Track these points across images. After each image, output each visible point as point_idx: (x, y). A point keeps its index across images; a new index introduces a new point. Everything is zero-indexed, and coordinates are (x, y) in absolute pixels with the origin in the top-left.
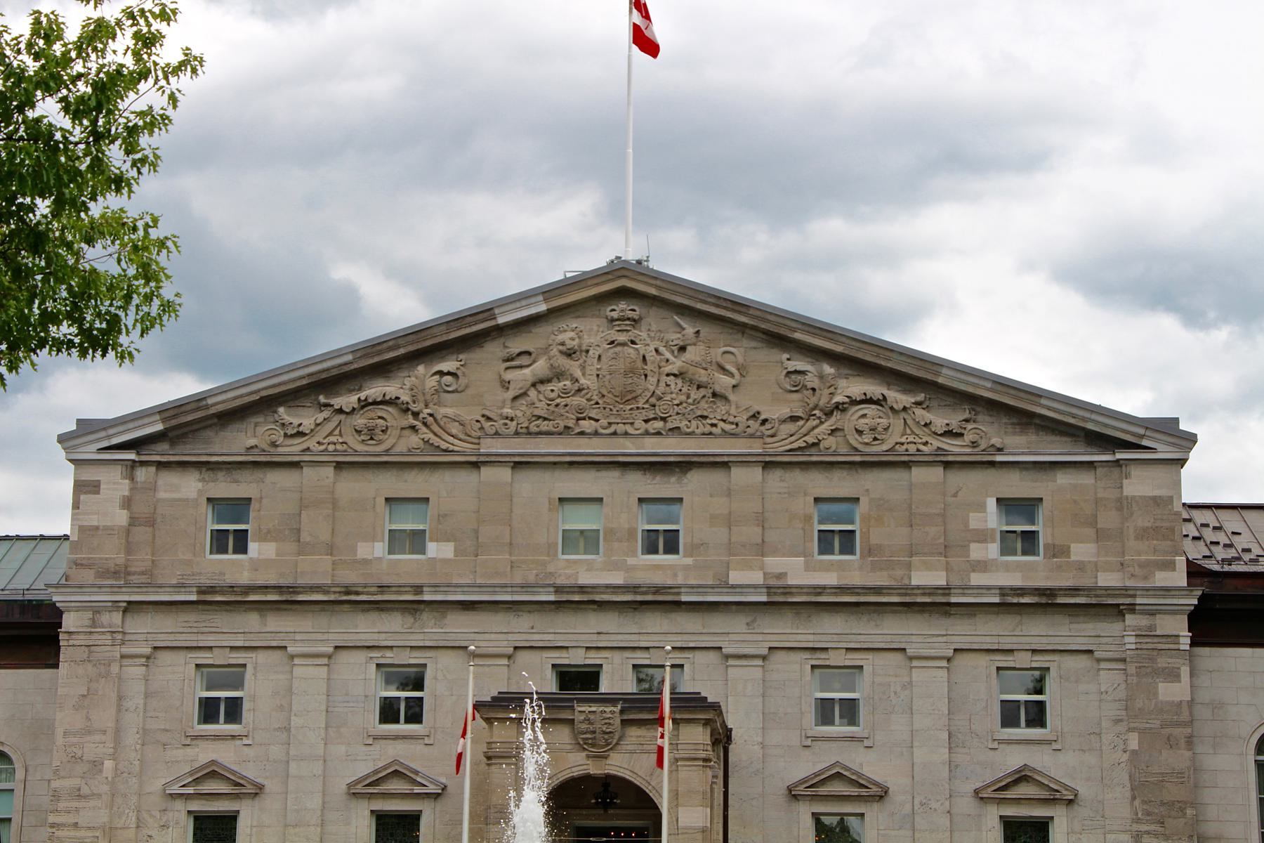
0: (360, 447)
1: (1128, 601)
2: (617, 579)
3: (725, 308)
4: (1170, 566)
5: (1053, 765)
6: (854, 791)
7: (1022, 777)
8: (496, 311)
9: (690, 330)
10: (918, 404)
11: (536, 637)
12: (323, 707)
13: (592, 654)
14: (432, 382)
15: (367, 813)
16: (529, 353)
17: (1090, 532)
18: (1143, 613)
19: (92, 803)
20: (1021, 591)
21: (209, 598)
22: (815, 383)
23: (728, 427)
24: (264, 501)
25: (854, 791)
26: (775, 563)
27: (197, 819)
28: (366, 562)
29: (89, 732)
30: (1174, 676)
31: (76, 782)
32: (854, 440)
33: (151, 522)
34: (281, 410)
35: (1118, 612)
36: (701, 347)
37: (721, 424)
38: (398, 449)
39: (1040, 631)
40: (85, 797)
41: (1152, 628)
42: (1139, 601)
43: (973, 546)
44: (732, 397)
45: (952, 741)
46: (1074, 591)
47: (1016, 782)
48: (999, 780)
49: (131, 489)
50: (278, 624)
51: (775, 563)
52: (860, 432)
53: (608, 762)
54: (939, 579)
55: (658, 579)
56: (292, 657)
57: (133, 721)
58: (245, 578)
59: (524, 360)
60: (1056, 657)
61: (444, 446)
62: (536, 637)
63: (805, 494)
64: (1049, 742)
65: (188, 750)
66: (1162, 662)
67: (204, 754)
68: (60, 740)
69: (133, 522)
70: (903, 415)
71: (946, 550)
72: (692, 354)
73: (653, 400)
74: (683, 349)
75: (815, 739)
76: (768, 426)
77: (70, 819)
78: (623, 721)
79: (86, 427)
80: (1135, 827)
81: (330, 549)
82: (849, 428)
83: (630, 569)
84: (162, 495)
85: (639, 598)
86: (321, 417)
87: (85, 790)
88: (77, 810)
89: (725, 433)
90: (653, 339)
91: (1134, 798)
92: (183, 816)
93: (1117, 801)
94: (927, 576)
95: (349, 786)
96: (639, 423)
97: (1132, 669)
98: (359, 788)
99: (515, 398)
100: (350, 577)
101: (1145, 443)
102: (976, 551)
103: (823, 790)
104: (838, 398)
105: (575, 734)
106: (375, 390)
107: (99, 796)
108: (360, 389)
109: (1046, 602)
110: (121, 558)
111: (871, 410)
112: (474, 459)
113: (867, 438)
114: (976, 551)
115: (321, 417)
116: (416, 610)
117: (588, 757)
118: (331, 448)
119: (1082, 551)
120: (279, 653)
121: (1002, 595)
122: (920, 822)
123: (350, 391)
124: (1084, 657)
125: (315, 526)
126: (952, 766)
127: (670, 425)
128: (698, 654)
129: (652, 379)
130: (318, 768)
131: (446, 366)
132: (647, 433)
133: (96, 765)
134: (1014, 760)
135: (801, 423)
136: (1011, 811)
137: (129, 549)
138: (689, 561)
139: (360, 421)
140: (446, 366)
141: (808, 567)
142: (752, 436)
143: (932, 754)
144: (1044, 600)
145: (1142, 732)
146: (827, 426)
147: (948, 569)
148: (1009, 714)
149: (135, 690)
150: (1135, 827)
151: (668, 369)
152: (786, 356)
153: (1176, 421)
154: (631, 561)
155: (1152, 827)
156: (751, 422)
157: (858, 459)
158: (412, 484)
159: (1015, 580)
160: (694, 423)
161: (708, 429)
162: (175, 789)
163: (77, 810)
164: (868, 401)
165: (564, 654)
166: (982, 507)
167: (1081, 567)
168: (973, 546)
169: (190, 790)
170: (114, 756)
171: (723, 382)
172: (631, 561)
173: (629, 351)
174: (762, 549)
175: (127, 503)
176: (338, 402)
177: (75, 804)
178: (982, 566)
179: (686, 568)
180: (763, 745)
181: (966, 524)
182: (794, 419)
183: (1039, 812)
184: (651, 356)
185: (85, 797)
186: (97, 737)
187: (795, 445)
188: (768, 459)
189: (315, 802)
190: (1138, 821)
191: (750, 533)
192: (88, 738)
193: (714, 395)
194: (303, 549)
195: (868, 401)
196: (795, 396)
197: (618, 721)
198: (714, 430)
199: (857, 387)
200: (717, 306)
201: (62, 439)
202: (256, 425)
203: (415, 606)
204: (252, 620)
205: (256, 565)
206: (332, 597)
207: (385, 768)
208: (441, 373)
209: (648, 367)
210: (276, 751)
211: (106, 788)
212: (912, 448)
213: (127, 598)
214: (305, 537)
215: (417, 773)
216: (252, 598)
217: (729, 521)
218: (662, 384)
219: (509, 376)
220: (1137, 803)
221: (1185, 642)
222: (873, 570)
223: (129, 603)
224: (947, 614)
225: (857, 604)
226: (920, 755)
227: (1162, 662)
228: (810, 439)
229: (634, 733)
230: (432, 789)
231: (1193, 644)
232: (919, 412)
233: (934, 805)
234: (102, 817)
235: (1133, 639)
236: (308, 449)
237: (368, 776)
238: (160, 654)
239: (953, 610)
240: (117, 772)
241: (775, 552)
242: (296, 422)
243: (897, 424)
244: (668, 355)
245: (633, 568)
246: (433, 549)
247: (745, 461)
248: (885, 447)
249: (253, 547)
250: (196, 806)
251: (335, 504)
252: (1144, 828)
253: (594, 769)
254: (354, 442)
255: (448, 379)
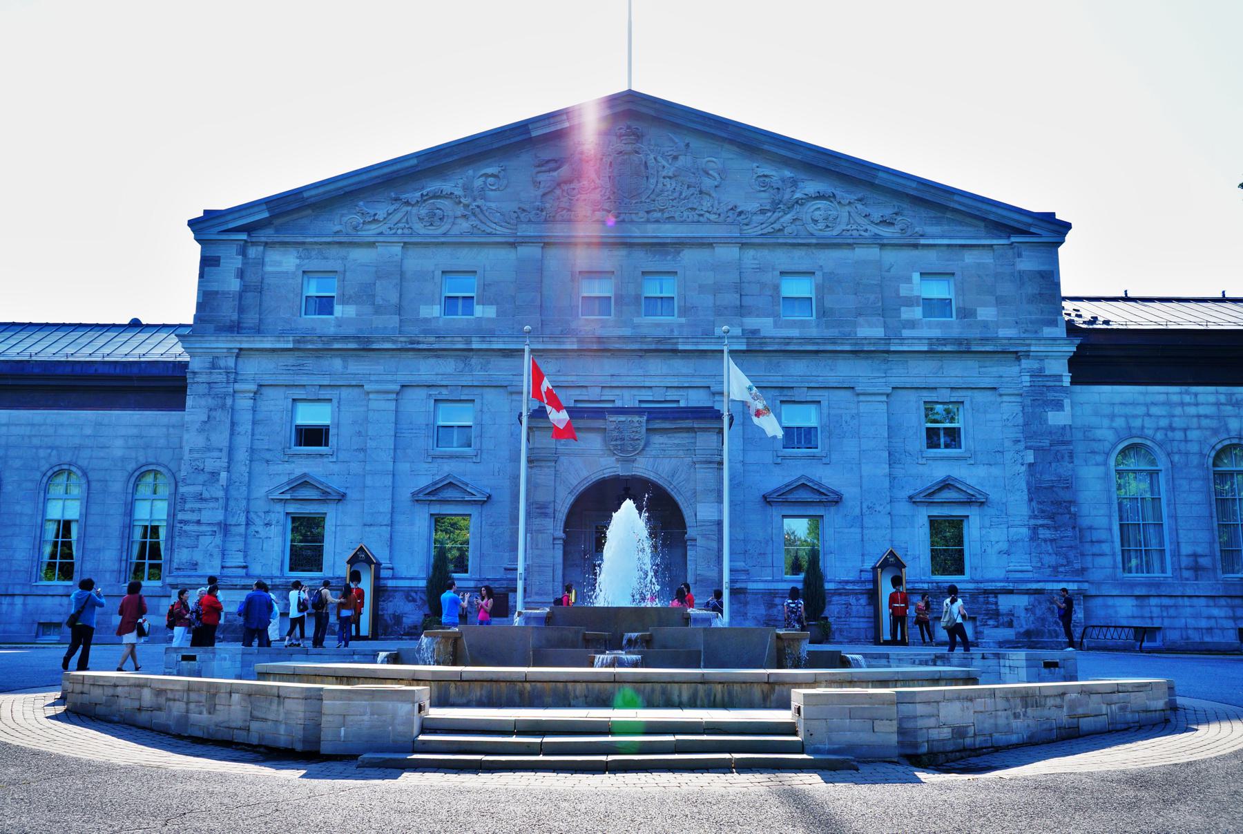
0: (422, 231)
1: (1025, 349)
2: (627, 332)
3: (710, 126)
4: (1053, 323)
5: (971, 476)
6: (817, 498)
7: (946, 485)
8: (530, 127)
9: (682, 145)
10: (860, 200)
11: (562, 378)
12: (392, 433)
13: (606, 392)
14: (479, 183)
15: (427, 516)
16: (555, 161)
17: (992, 299)
18: (1036, 358)
19: (211, 505)
20: (944, 341)
21: (302, 346)
22: (780, 184)
23: (713, 217)
24: (348, 274)
25: (817, 498)
26: (752, 322)
27: (294, 520)
28: (426, 320)
29: (208, 449)
30: (1059, 406)
31: (198, 488)
32: (811, 228)
33: (260, 289)
34: (361, 203)
35: (1017, 356)
36: (689, 158)
37: (707, 215)
38: (452, 232)
39: (957, 371)
40: (206, 500)
41: (1042, 369)
42: (1033, 349)
43: (903, 309)
44: (714, 195)
45: (893, 460)
46: (985, 340)
47: (940, 489)
48: (928, 488)
49: (243, 264)
50: (358, 367)
51: (752, 322)
52: (815, 221)
53: (636, 465)
54: (879, 332)
55: (660, 333)
56: (368, 393)
57: (243, 442)
58: (332, 330)
59: (552, 165)
60: (969, 393)
61: (489, 230)
62: (562, 378)
63: (774, 269)
64: (965, 459)
65: (286, 465)
66: (1051, 396)
67: (299, 468)
68: (187, 456)
69: (245, 289)
70: (847, 208)
71: (883, 312)
72: (682, 161)
73: (653, 197)
74: (675, 158)
75: (784, 458)
76: (743, 216)
77: (194, 517)
78: (648, 430)
79: (210, 216)
80: (1033, 522)
81: (399, 309)
82: (807, 218)
83: (635, 327)
84: (268, 269)
85: (645, 347)
86: (394, 207)
87: (206, 495)
88: (200, 510)
89: (709, 221)
90: (652, 151)
91: (1031, 500)
92: (282, 516)
93: (1019, 505)
94: (870, 331)
95: (413, 494)
96: (642, 214)
97: (1028, 401)
98: (421, 497)
99: (544, 195)
100: (413, 330)
101: (1032, 230)
102: (907, 314)
103: (791, 497)
104: (798, 195)
105: (604, 440)
106: (434, 186)
107: (217, 499)
108: (423, 188)
109: (963, 350)
110: (235, 317)
111: (822, 204)
112: (511, 240)
113: (821, 226)
114: (907, 314)
115: (392, 208)
116: (466, 357)
117: (617, 460)
118: (400, 232)
119: (986, 313)
120: (357, 390)
121: (931, 344)
122: (868, 522)
123: (416, 190)
124: (989, 393)
125: (387, 293)
126: (892, 477)
127: (666, 215)
128: (691, 392)
129: (653, 181)
130: (388, 481)
131: (489, 171)
132: (648, 221)
133: (214, 475)
134: (940, 472)
135: (769, 214)
136: (936, 511)
137: (241, 310)
138: (683, 320)
139: (423, 212)
140: (489, 171)
141: (776, 325)
142: (732, 224)
143: (877, 470)
144: (963, 348)
145: (1037, 450)
146: (789, 217)
147: (886, 326)
148: (932, 438)
149: (245, 419)
150: (1033, 522)
151: (664, 174)
152: (755, 165)
153: (1054, 214)
154: (636, 320)
155: (1046, 522)
156: (730, 214)
157: (814, 241)
158: (465, 258)
159: (936, 333)
160: (685, 214)
161: (696, 218)
162: (276, 495)
163: (200, 510)
164: (820, 197)
165: (584, 391)
166: (909, 280)
167: (985, 325)
168: (903, 309)
169: (288, 496)
170: (228, 470)
171: (707, 183)
172: (636, 320)
173: (635, 158)
174: (742, 310)
175: (241, 274)
176: (404, 196)
177: (198, 505)
178: (912, 324)
179: (681, 326)
180: (743, 463)
181: (897, 291)
182: (763, 212)
183: (957, 512)
184: (651, 163)
185: (206, 500)
186: (216, 454)
187: (765, 231)
188: (744, 241)
189: (386, 507)
190: (1035, 517)
191: (731, 298)
192: (208, 454)
193: (701, 192)
194: (378, 310)
195: (820, 197)
196: (763, 195)
197: (644, 430)
198: (701, 219)
199: (812, 186)
200: (704, 125)
201: (192, 223)
202: (342, 215)
203: (466, 353)
204: (337, 364)
205: (340, 323)
206: (399, 346)
207: (441, 481)
208: (487, 176)
209: (651, 171)
210: (355, 467)
211: (221, 494)
212: (855, 233)
213: (238, 346)
214: (379, 301)
215: (467, 485)
216: (336, 346)
217: (717, 289)
218: (660, 186)
219: (542, 177)
220: (1034, 504)
221: (1067, 381)
222: (827, 327)
223: (241, 349)
224: (886, 361)
225: (817, 352)
226: (867, 469)
227: (1051, 396)
228: (777, 226)
229: (658, 440)
230: (479, 497)
231: (1072, 383)
232: (859, 206)
233: (878, 508)
234: (219, 516)
235: (1028, 379)
236: (381, 233)
237: (427, 487)
238: (264, 390)
239: (891, 357)
240: (229, 479)
241: (749, 314)
242: (372, 212)
243: (844, 213)
244: (665, 163)
245: (638, 326)
246: (479, 311)
247: (726, 241)
248: (835, 233)
249: (338, 310)
250: (292, 508)
251: (402, 274)
252: (1040, 522)
253: (620, 470)
254: (419, 227)
255: (491, 180)
